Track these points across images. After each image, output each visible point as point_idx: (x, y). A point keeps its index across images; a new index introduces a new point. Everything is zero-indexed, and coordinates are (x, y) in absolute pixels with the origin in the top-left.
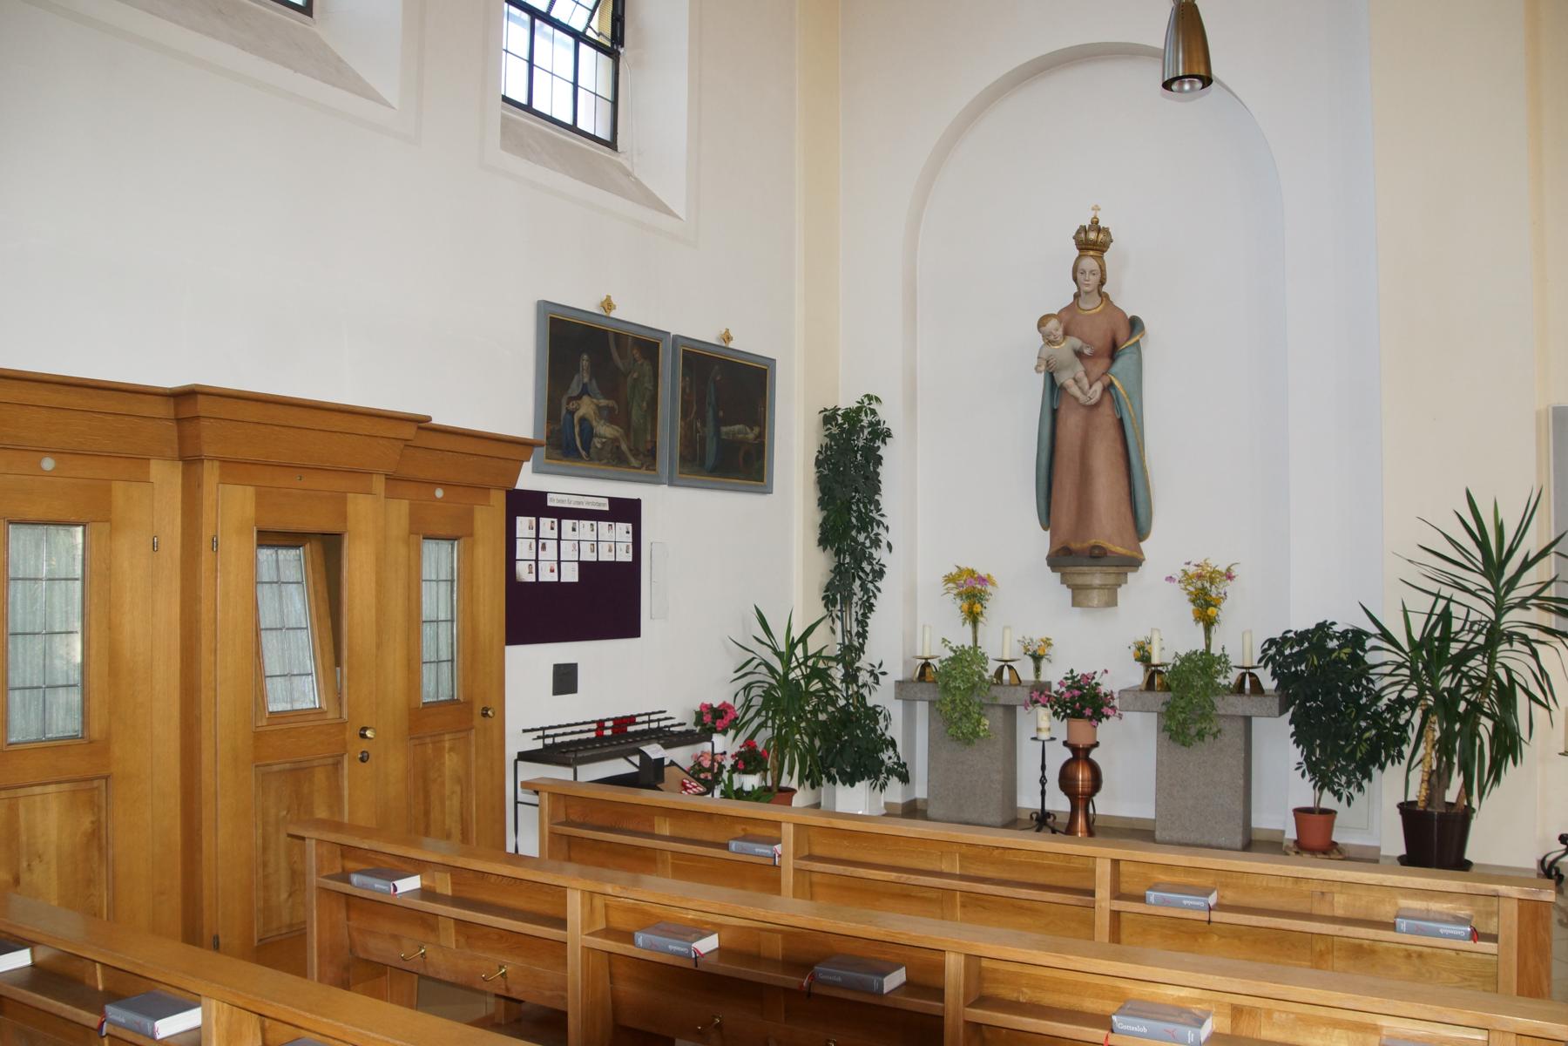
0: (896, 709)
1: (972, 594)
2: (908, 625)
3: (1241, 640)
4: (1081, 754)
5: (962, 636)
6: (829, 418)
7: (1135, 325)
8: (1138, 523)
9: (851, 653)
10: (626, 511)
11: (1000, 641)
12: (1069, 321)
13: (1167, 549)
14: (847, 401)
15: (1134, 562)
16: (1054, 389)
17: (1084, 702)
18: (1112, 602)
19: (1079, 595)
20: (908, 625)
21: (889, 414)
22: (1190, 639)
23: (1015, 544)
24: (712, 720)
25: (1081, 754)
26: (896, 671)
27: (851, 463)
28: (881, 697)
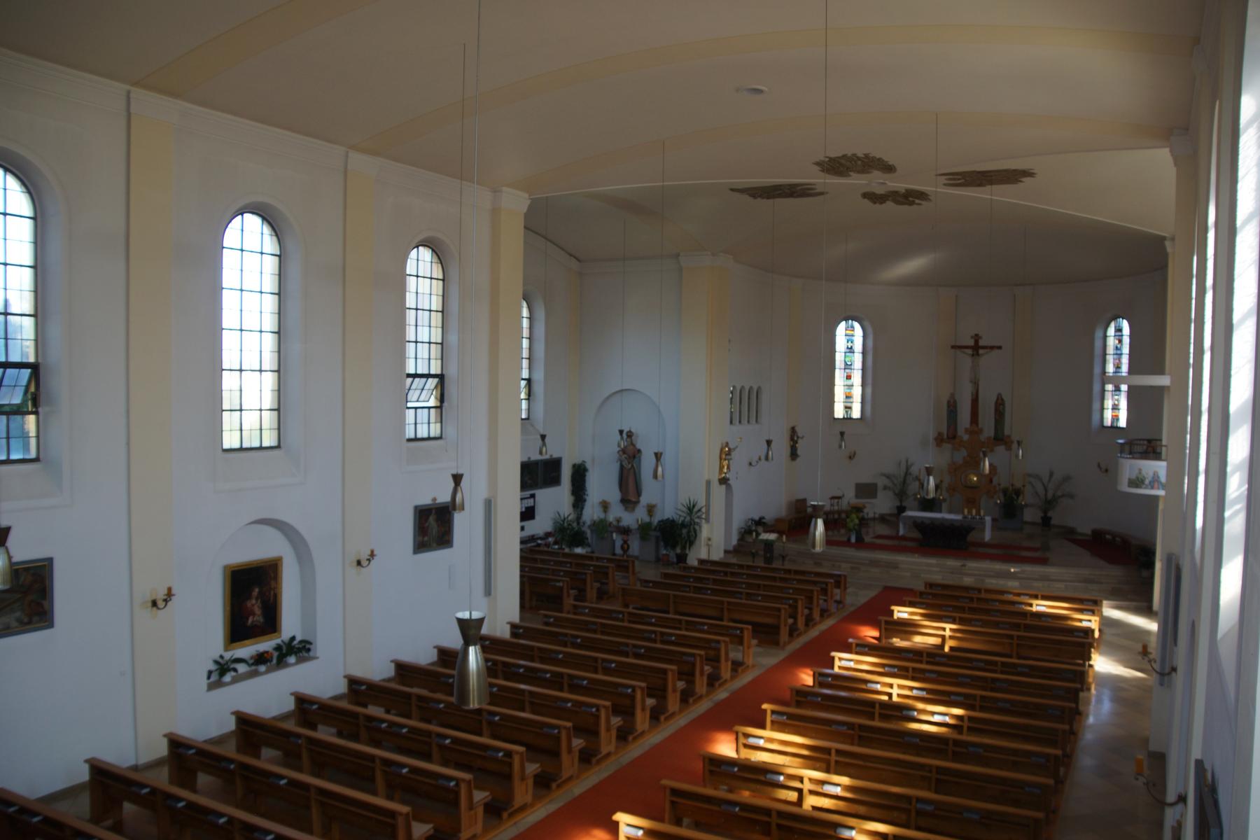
0: (589, 532)
1: (605, 506)
2: (591, 512)
3: (656, 520)
4: (625, 542)
5: (602, 516)
6: (574, 466)
7: (639, 451)
8: (639, 494)
9: (579, 518)
10: (533, 496)
11: (611, 518)
12: (624, 451)
13: (645, 499)
14: (578, 461)
15: (638, 502)
16: (622, 467)
17: (625, 531)
18: (633, 510)
19: (626, 509)
20: (591, 512)
21: (588, 465)
22: (647, 519)
23: (614, 495)
24: (548, 535)
25: (625, 542)
26: (588, 523)
27: (579, 474)
28: (585, 529)
